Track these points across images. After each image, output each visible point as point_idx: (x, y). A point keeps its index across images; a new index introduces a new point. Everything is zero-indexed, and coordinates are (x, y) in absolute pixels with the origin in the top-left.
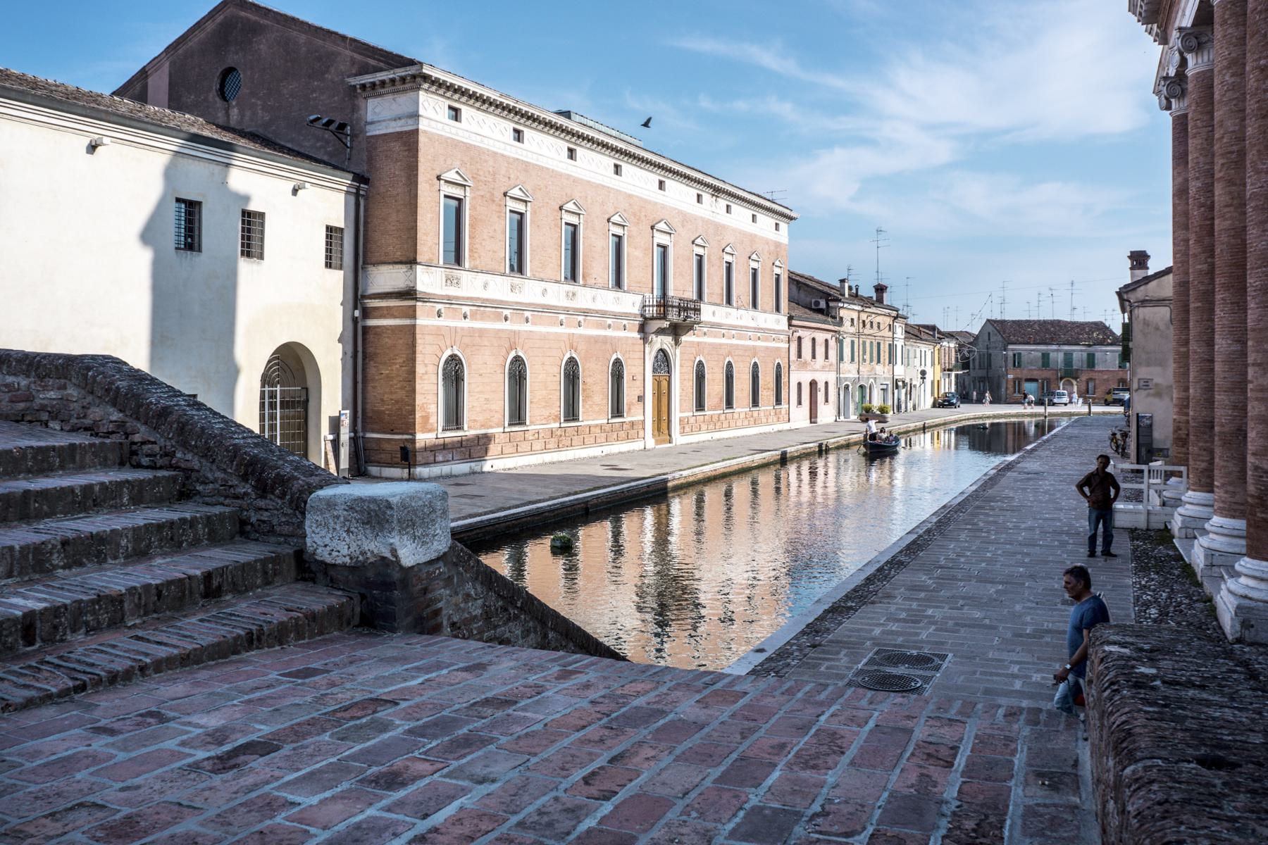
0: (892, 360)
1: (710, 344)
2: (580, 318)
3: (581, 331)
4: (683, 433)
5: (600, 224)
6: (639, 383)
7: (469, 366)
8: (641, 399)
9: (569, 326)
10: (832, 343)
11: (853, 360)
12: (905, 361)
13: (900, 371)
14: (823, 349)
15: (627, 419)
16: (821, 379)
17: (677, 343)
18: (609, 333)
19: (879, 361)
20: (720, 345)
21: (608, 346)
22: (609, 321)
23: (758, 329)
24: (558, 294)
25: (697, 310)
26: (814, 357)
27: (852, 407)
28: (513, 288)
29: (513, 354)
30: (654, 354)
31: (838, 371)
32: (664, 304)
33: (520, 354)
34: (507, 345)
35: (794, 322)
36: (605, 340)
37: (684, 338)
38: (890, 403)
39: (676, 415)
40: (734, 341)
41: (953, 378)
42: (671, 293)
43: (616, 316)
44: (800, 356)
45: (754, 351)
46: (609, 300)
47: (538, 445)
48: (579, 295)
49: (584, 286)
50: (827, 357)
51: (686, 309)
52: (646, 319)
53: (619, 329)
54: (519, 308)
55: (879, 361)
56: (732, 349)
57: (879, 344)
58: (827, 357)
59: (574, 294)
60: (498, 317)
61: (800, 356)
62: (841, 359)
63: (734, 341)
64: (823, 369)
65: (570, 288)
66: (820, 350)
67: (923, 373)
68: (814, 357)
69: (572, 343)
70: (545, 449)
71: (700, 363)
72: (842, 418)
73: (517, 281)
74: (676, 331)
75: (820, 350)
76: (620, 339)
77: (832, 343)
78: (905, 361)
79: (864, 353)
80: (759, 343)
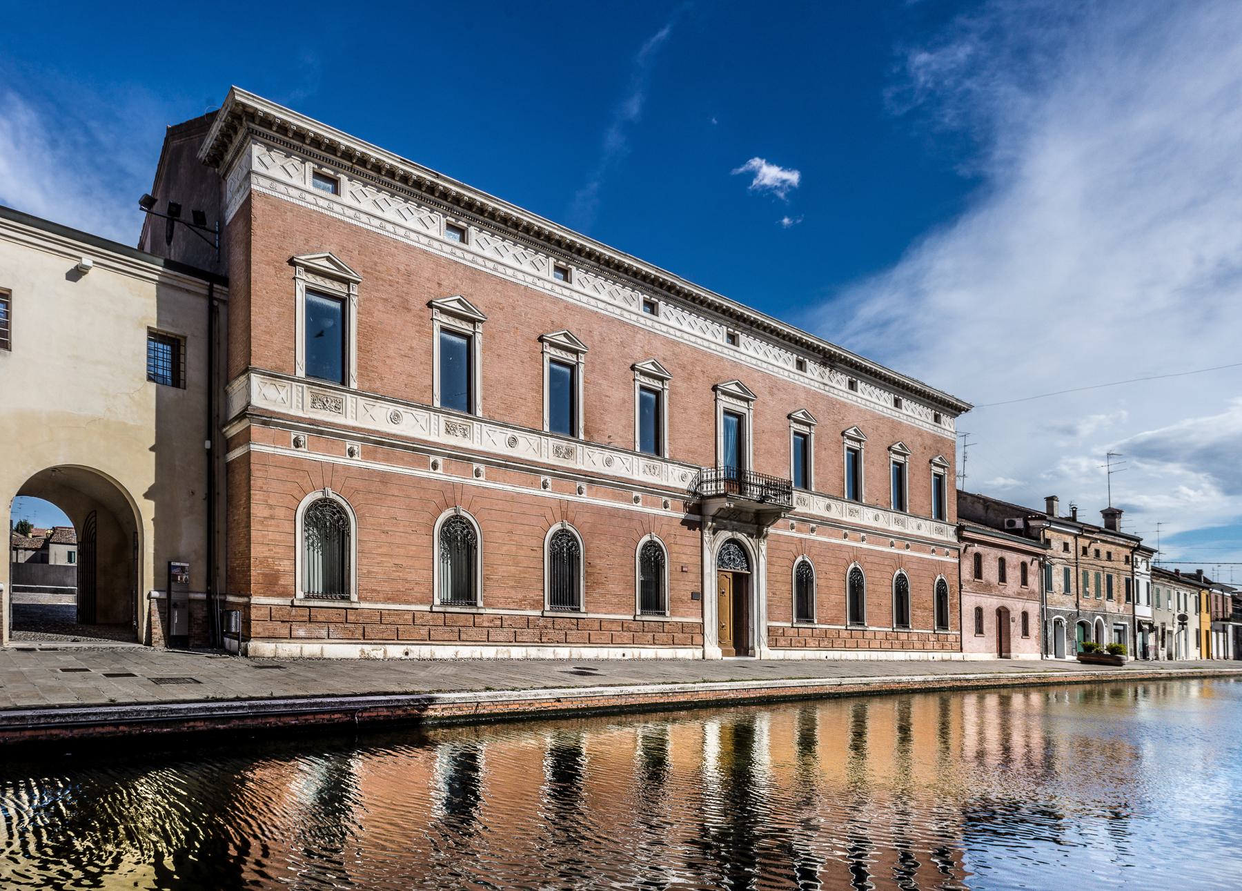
0: (1131, 594)
1: (820, 543)
2: (584, 486)
3: (584, 499)
5: (619, 370)
6: (693, 577)
9: (561, 491)
10: (1034, 568)
11: (1067, 590)
12: (1153, 599)
13: (1144, 611)
14: (1019, 573)
16: (1016, 607)
17: (759, 534)
18: (637, 507)
19: (1110, 596)
20: (840, 546)
21: (636, 524)
22: (635, 494)
23: (902, 537)
24: (538, 448)
26: (1003, 578)
27: (1067, 645)
30: (719, 543)
31: (1043, 601)
32: (737, 478)
35: (966, 534)
36: (629, 515)
37: (771, 530)
38: (1130, 647)
40: (864, 545)
41: (1230, 629)
42: (750, 465)
43: (647, 489)
44: (978, 573)
45: (899, 561)
46: (635, 468)
50: (1024, 582)
52: (703, 497)
53: (654, 505)
54: (461, 458)
55: (1110, 596)
56: (857, 554)
57: (1109, 578)
58: (1024, 582)
60: (422, 464)
61: (978, 573)
62: (1049, 587)
63: (864, 545)
64: (1019, 595)
66: (1013, 574)
67: (1183, 619)
68: (1003, 578)
71: (804, 563)
72: (1052, 657)
74: (758, 521)
75: (1013, 574)
77: (1034, 568)
78: (1153, 599)
79: (1086, 584)
80: (907, 552)
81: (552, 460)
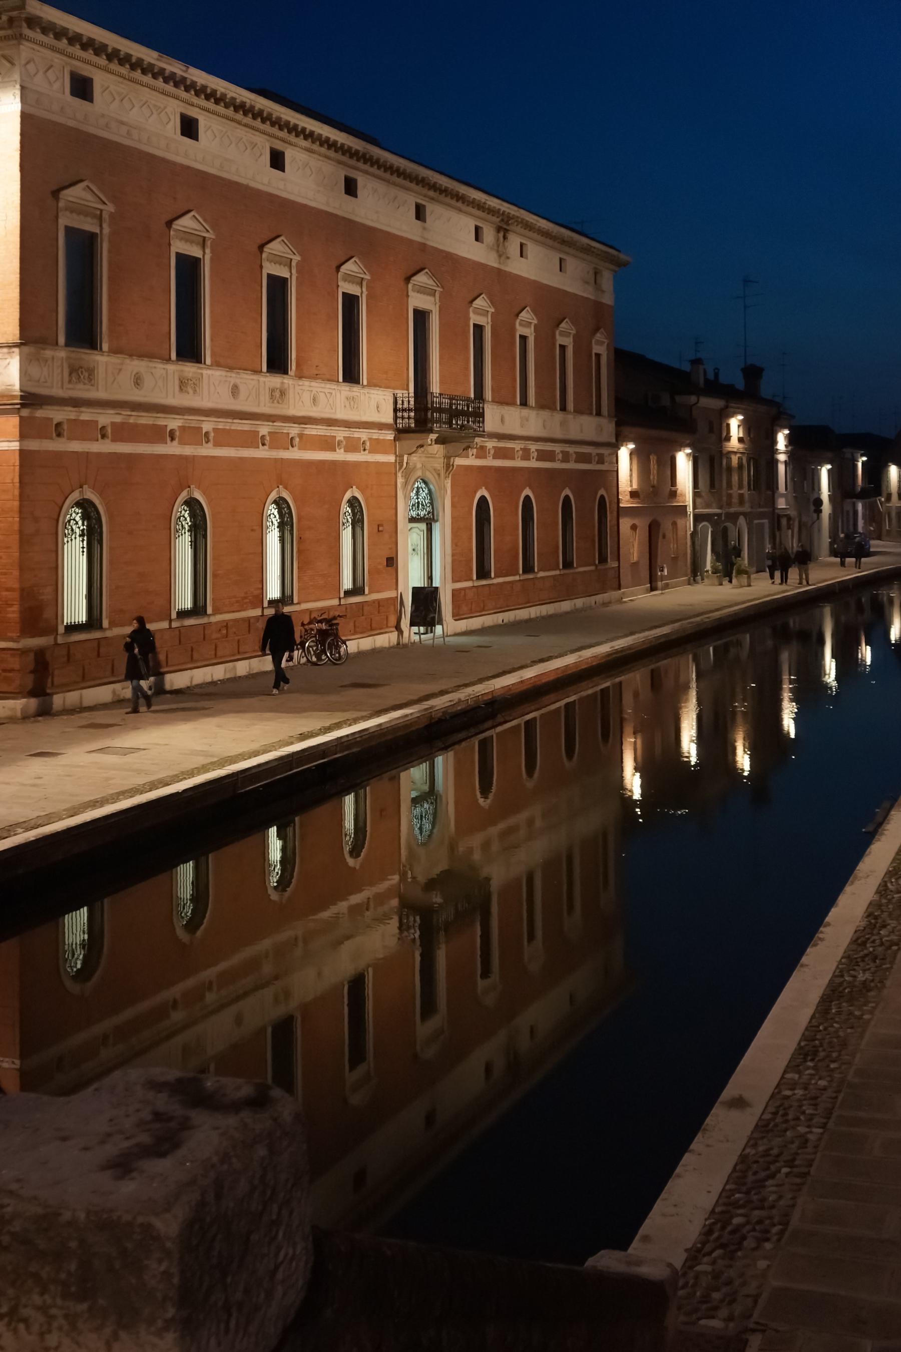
25: (479, 415)
48: (291, 394)
49: (300, 376)
51: (458, 414)
59: (283, 393)
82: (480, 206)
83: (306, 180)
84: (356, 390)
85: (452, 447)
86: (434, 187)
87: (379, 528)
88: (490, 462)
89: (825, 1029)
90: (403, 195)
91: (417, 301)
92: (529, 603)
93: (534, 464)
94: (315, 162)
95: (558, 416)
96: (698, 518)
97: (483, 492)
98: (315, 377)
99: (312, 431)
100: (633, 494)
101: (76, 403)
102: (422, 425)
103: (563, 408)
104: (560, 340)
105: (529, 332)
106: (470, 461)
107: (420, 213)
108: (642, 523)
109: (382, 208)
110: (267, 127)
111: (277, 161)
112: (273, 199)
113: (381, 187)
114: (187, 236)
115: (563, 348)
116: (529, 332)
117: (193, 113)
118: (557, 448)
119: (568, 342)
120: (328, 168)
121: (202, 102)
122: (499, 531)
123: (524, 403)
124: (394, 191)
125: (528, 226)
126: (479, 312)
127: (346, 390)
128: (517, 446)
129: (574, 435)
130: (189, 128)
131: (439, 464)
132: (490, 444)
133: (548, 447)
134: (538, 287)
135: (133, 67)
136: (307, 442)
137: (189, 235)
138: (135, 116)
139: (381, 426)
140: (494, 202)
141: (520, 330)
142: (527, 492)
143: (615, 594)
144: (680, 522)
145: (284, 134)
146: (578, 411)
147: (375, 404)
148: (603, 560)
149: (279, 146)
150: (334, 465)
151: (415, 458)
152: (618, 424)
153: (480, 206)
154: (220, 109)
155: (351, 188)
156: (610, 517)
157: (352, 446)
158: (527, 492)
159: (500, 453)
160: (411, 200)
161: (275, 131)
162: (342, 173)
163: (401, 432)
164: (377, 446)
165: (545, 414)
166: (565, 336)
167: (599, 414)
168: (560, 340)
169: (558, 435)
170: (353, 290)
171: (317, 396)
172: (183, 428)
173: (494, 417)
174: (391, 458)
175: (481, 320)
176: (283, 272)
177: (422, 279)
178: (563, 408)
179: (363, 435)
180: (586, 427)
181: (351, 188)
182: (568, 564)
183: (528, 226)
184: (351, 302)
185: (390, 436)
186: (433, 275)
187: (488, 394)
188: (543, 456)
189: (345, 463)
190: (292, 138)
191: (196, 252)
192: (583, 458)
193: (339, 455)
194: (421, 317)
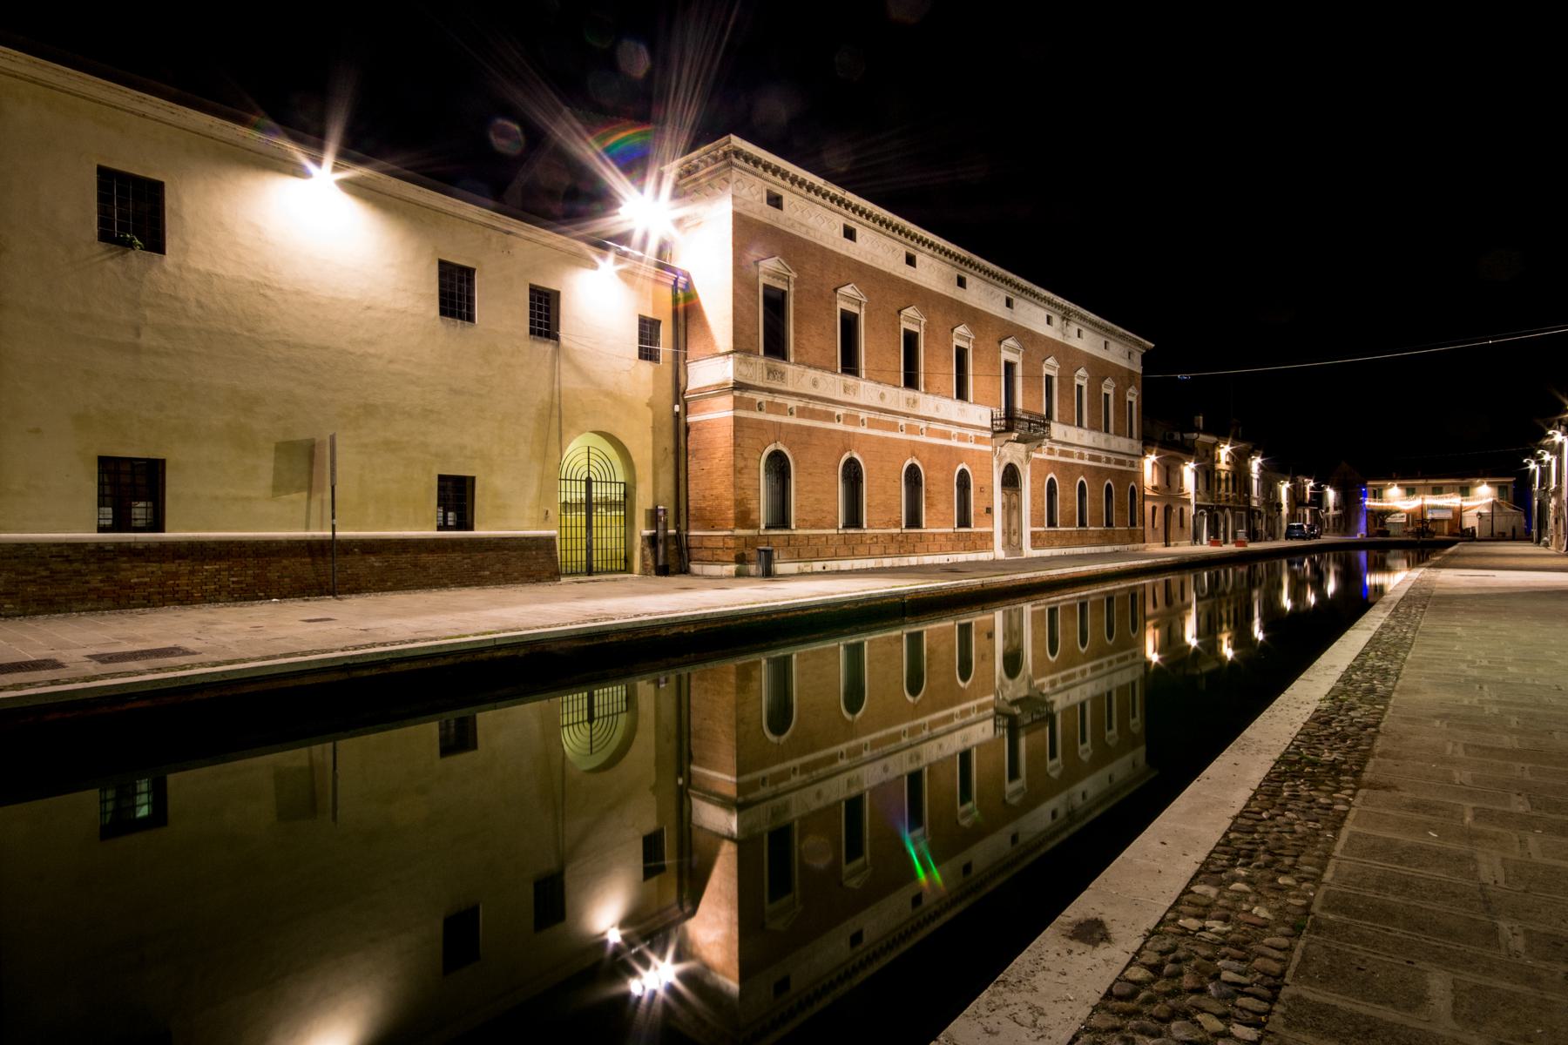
4: (1034, 547)
7: (797, 463)
8: (989, 510)
15: (973, 529)
28: (846, 389)
29: (846, 456)
33: (856, 456)
34: (840, 446)
39: (1027, 530)
47: (876, 550)
59: (915, 402)
65: (910, 393)
69: (914, 449)
70: (885, 554)
73: (850, 380)
76: (965, 450)
81: (903, 408)
82: (1050, 302)
83: (932, 273)
84: (965, 405)
85: (1030, 445)
86: (1017, 286)
87: (981, 490)
88: (1056, 458)
89: (1271, 818)
90: (997, 291)
91: (1006, 355)
92: (1083, 545)
93: (1086, 462)
94: (936, 263)
95: (1103, 436)
96: (1198, 507)
97: (1051, 475)
98: (937, 394)
99: (934, 426)
100: (1154, 488)
101: (771, 391)
102: (1009, 429)
103: (1107, 431)
104: (1105, 390)
105: (1084, 383)
106: (1042, 455)
107: (1009, 303)
108: (1160, 506)
109: (982, 295)
110: (902, 237)
111: (911, 260)
112: (907, 283)
113: (983, 285)
114: (848, 298)
115: (1107, 396)
116: (1084, 383)
117: (852, 224)
118: (1103, 455)
119: (1111, 392)
120: (946, 269)
121: (856, 216)
122: (1063, 500)
123: (1080, 425)
124: (991, 288)
125: (1083, 318)
126: (1049, 366)
127: (958, 404)
128: (1075, 450)
129: (1114, 447)
130: (849, 234)
131: (1022, 456)
132: (1057, 447)
133: (1097, 453)
134: (1088, 355)
135: (809, 190)
136: (930, 432)
137: (849, 297)
138: (811, 221)
139: (983, 428)
140: (1059, 300)
141: (1077, 381)
142: (1082, 478)
143: (1141, 546)
144: (1186, 508)
145: (914, 243)
146: (1117, 434)
147: (979, 414)
148: (1133, 524)
149: (912, 251)
150: (950, 448)
151: (1004, 450)
152: (1144, 445)
153: (1050, 302)
154: (870, 222)
155: (961, 282)
156: (1138, 500)
157: (962, 438)
158: (1082, 478)
159: (1062, 453)
160: (1003, 294)
161: (908, 240)
162: (956, 273)
163: (995, 433)
164: (978, 440)
165: (1095, 433)
166: (1108, 388)
167: (1131, 437)
168: (1105, 390)
169: (1103, 446)
170: (964, 344)
171: (937, 405)
172: (846, 415)
173: (1057, 430)
174: (990, 449)
175: (1051, 373)
176: (915, 329)
177: (1010, 342)
178: (1107, 431)
179: (971, 433)
180: (1123, 444)
181: (961, 282)
182: (1109, 524)
183: (1083, 318)
184: (961, 353)
185: (988, 435)
186: (1019, 341)
187: (1056, 417)
188: (1092, 458)
189: (957, 449)
190: (920, 246)
191: (855, 309)
192: (1118, 462)
193: (954, 443)
194: (1009, 367)
